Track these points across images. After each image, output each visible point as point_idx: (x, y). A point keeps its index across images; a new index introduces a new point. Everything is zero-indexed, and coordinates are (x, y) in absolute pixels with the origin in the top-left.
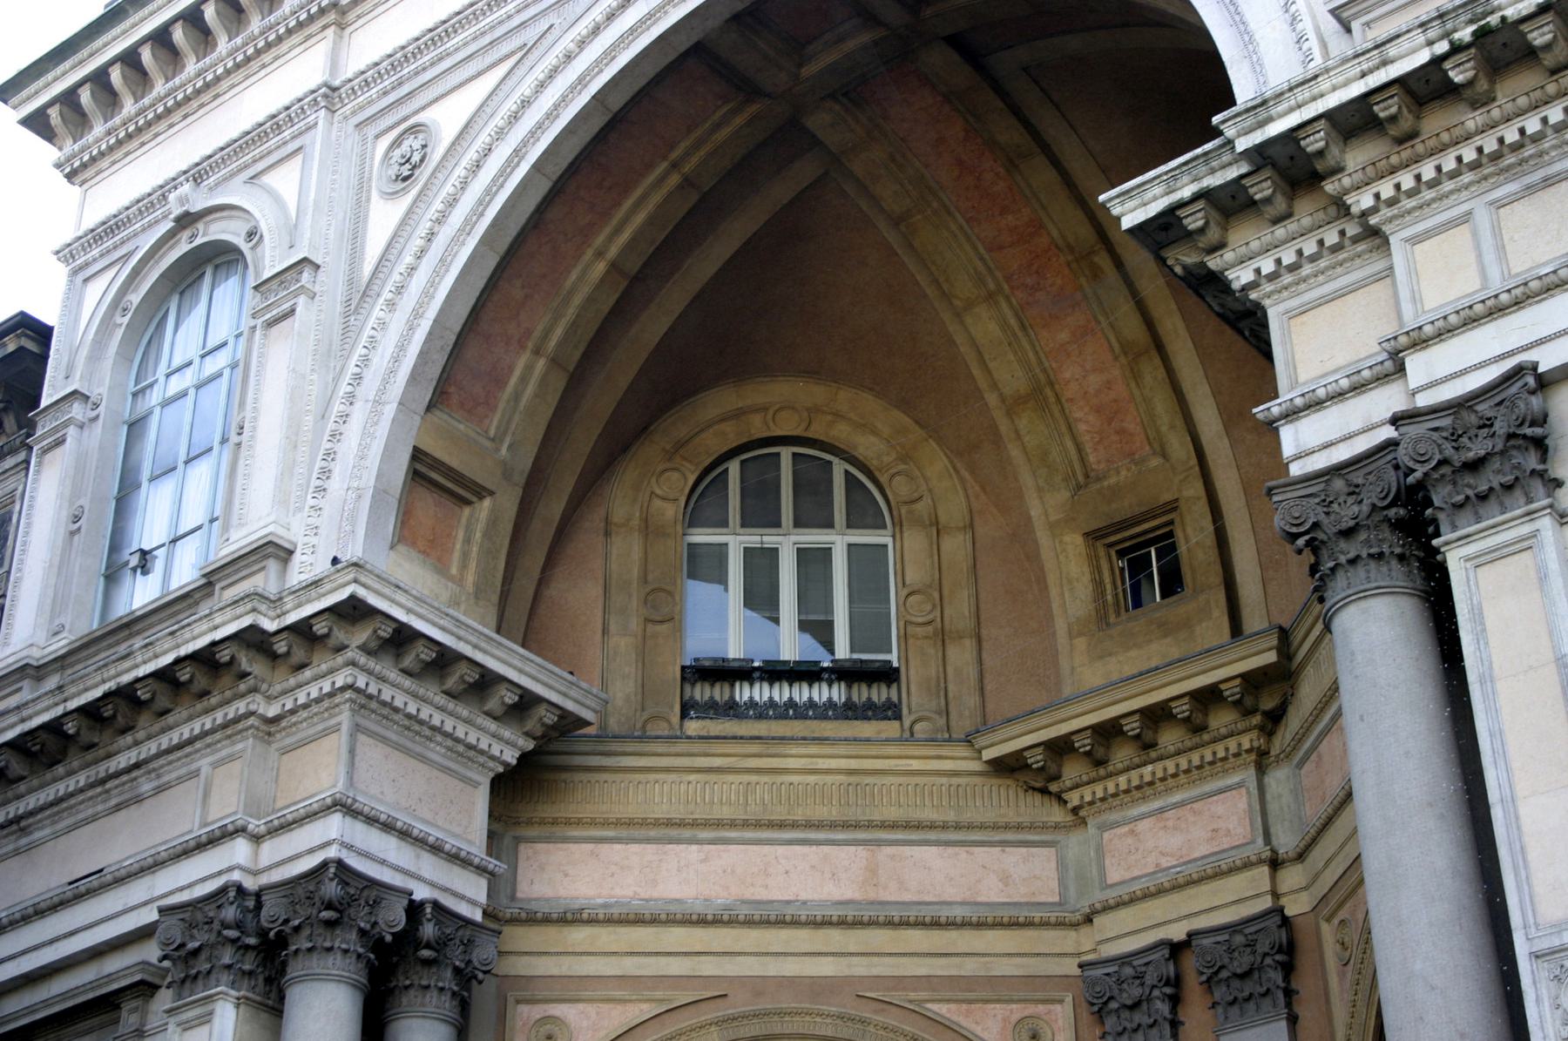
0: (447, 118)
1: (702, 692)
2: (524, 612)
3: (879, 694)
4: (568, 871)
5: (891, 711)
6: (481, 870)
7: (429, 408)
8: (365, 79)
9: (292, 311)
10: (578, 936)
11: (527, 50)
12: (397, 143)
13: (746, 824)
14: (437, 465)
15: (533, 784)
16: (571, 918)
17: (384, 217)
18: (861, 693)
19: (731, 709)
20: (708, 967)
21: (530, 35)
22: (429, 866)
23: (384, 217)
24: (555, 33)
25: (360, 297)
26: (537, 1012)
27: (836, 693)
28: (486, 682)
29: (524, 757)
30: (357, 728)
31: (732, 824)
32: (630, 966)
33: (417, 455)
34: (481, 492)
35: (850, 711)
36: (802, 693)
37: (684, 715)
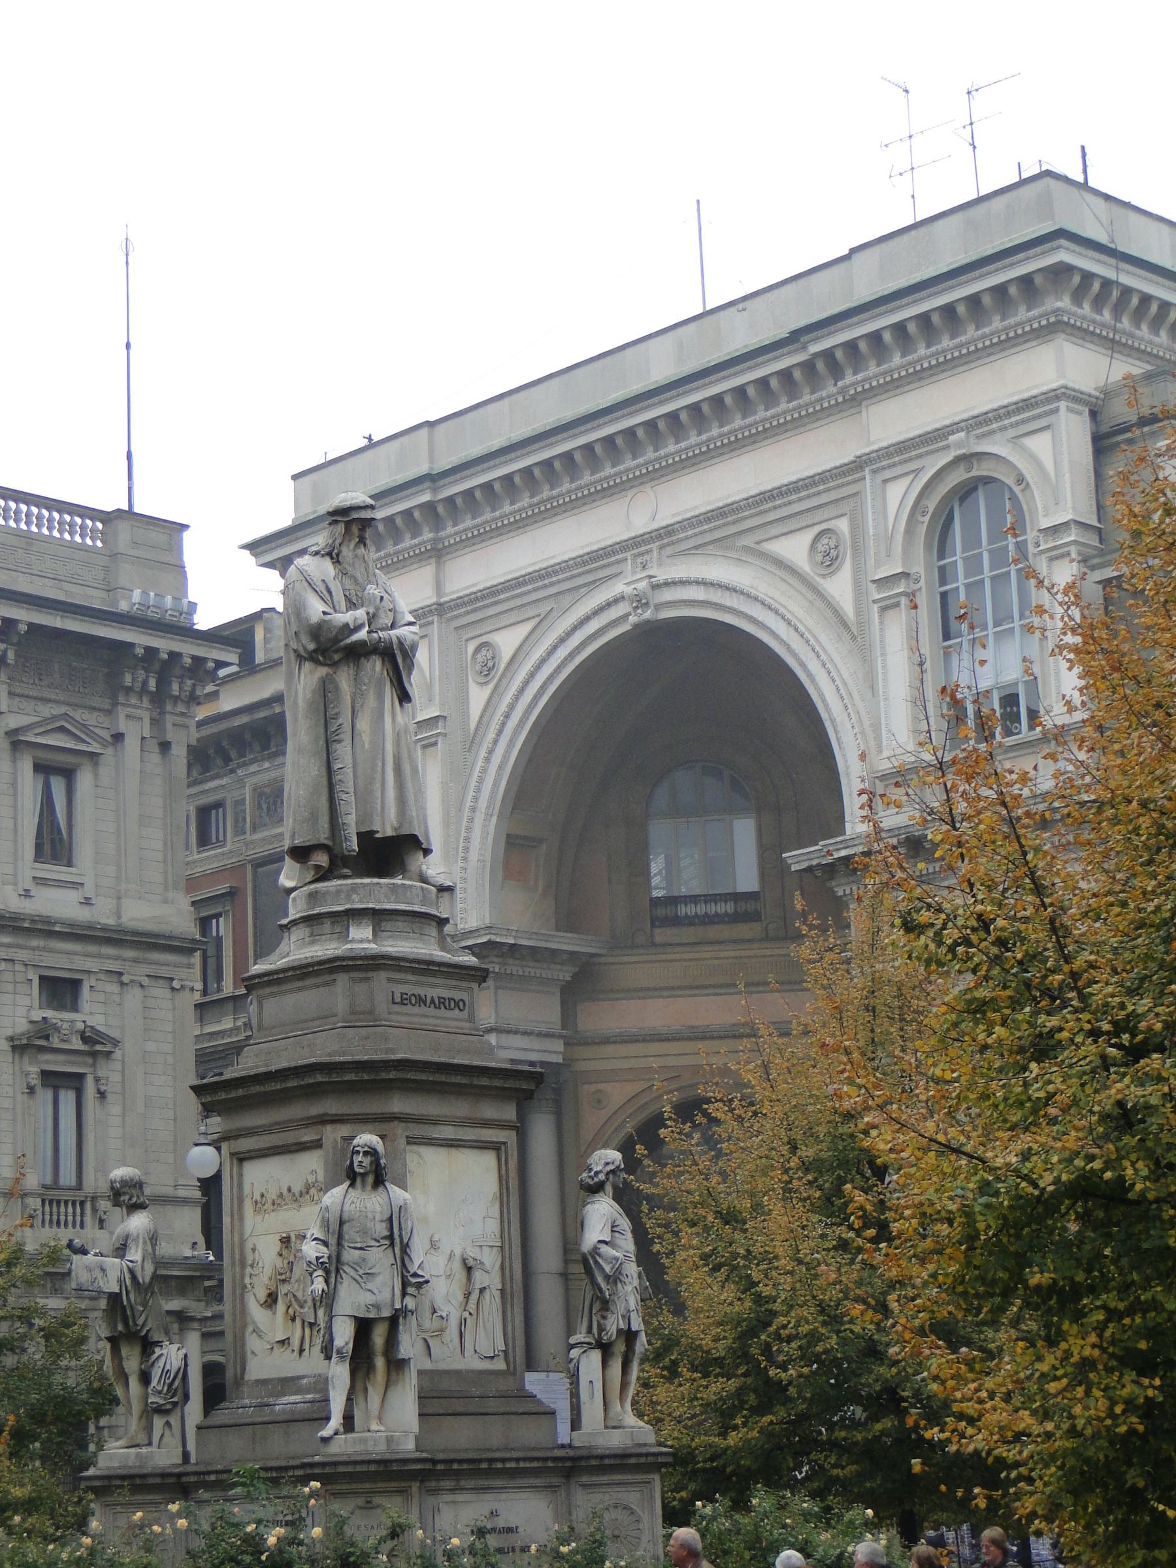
0: (507, 642)
1: (661, 912)
2: (568, 920)
3: (750, 906)
4: (601, 1018)
5: (755, 917)
6: (560, 1036)
7: (512, 813)
8: (460, 602)
9: (435, 744)
10: (609, 1050)
11: (542, 621)
12: (478, 650)
13: (686, 988)
14: (517, 837)
15: (582, 983)
16: (606, 1041)
17: (478, 696)
18: (743, 907)
19: (677, 922)
20: (672, 1062)
21: (544, 608)
22: (536, 1043)
23: (478, 696)
24: (554, 614)
25: (471, 744)
26: (593, 1088)
27: (729, 908)
28: (554, 952)
29: (575, 976)
30: (497, 988)
31: (680, 988)
32: (633, 1063)
33: (509, 836)
34: (541, 841)
35: (737, 918)
36: (712, 909)
37: (653, 925)
